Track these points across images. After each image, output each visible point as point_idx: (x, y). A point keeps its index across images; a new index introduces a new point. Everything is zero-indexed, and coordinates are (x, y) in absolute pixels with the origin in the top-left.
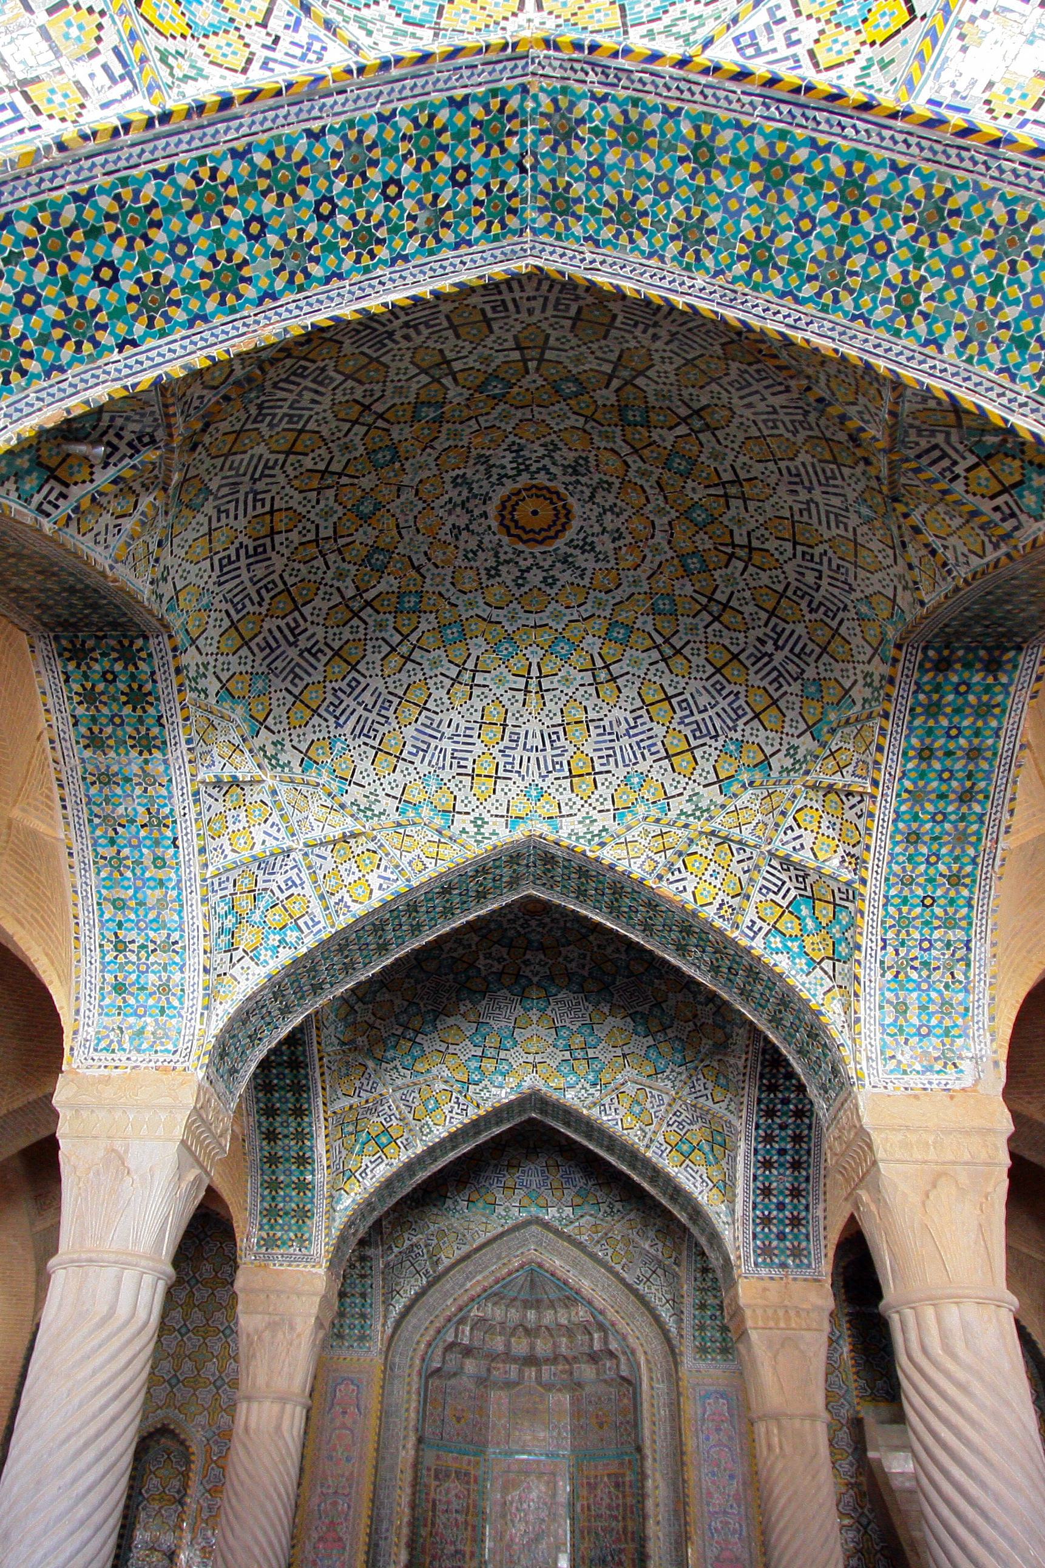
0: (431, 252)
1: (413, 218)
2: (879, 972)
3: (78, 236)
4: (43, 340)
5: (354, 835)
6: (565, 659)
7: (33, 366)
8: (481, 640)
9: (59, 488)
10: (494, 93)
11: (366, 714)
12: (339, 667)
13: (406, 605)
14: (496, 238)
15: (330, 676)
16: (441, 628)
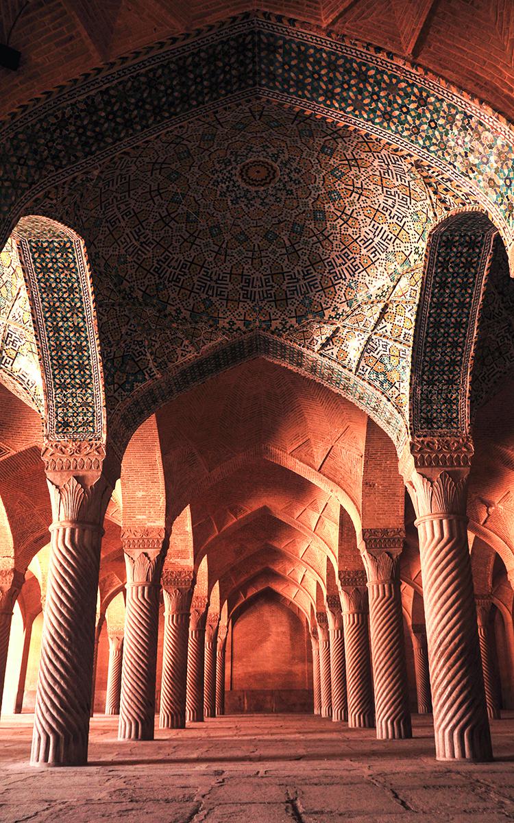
0: (77, 270)
1: (66, 275)
2: (467, 179)
3: (60, 361)
4: (83, 376)
5: (386, 306)
6: (343, 174)
7: (88, 381)
8: (326, 206)
9: (147, 369)
10: (31, 250)
11: (346, 266)
12: (319, 266)
13: (297, 230)
14: (73, 250)
15: (322, 272)
16: (315, 219)
